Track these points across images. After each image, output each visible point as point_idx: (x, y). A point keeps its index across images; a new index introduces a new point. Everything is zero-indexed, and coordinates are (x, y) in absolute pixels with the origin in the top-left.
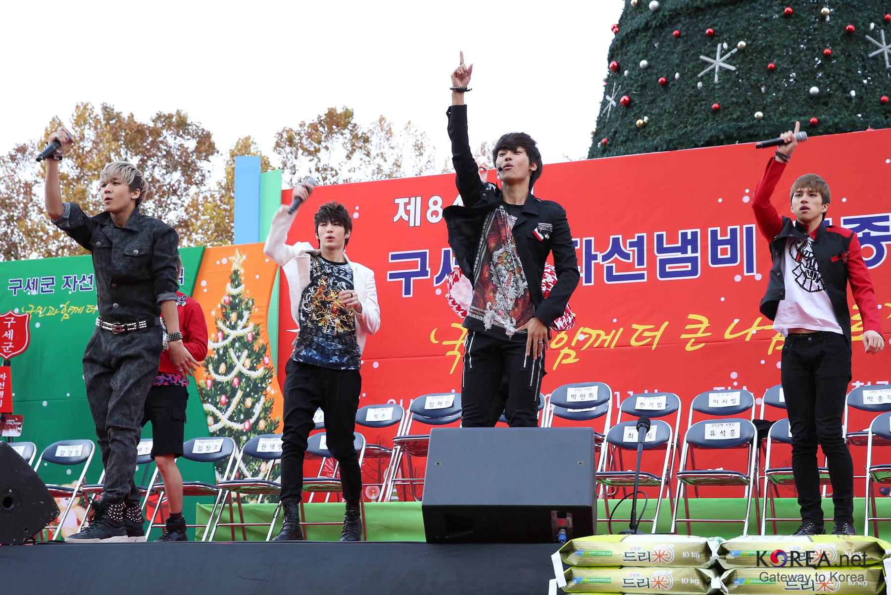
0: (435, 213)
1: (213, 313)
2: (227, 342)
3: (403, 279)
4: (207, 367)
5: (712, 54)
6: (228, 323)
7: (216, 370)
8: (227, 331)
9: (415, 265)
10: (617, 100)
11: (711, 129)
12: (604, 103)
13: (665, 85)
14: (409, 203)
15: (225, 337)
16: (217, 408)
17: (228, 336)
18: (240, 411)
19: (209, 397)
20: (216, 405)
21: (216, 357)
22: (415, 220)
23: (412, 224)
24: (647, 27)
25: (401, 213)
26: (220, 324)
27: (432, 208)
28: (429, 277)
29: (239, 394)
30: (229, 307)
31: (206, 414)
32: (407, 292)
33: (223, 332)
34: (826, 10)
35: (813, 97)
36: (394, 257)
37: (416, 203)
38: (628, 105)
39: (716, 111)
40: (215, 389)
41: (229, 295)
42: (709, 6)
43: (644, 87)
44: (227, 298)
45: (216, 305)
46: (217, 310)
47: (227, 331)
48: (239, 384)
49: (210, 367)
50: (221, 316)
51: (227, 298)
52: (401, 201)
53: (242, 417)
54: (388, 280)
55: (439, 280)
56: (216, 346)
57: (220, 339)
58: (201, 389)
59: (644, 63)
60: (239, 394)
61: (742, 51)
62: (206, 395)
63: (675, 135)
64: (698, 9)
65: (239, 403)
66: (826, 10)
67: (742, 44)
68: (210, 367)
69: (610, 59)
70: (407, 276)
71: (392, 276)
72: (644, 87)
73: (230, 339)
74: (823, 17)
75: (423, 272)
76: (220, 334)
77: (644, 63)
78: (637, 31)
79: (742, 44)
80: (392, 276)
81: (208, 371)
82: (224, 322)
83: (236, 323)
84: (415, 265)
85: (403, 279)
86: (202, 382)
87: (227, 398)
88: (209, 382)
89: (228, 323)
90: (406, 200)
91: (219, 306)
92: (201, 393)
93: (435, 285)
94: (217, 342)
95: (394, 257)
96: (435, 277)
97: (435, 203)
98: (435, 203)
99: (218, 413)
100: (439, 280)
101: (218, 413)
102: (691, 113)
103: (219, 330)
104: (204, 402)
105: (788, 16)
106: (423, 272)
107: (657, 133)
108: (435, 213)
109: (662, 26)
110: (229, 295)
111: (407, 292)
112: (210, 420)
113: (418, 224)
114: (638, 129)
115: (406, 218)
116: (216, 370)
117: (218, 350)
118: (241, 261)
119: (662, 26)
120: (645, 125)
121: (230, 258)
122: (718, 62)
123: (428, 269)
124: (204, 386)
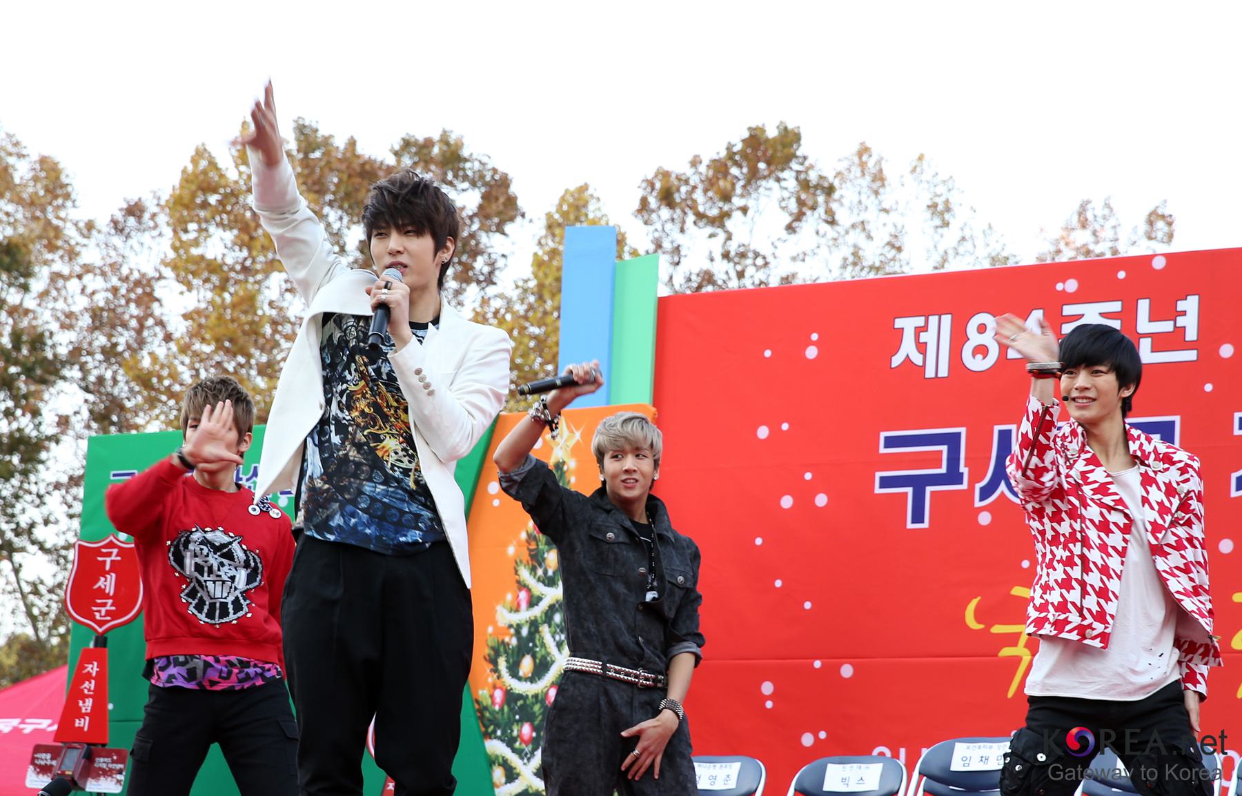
0: (982, 350)
1: (511, 550)
2: (537, 611)
3: (910, 490)
4: (494, 662)
6: (540, 572)
7: (514, 670)
8: (538, 588)
9: (935, 460)
14: (925, 328)
15: (533, 601)
16: (514, 750)
17: (540, 599)
19: (497, 726)
20: (510, 742)
21: (514, 642)
22: (937, 365)
23: (930, 373)
25: (908, 348)
26: (525, 574)
27: (975, 339)
28: (964, 486)
31: (492, 761)
32: (918, 518)
33: (529, 590)
36: (890, 442)
37: (940, 328)
40: (511, 710)
45: (519, 532)
46: (519, 544)
47: (538, 588)
49: (502, 663)
50: (525, 556)
52: (907, 324)
54: (878, 490)
55: (986, 492)
56: (515, 618)
57: (524, 605)
58: (482, 710)
62: (491, 722)
68: (502, 663)
70: (919, 484)
71: (885, 482)
73: (544, 605)
75: (953, 476)
76: (523, 595)
80: (885, 482)
81: (496, 670)
82: (533, 570)
84: (935, 460)
85: (910, 490)
86: (483, 694)
88: (498, 695)
89: (540, 572)
90: (920, 321)
91: (524, 536)
92: (482, 718)
93: (978, 504)
94: (517, 610)
95: (890, 442)
96: (978, 486)
97: (982, 329)
98: (982, 329)
99: (514, 760)
100: (986, 492)
101: (514, 760)
103: (522, 586)
104: (488, 735)
106: (953, 476)
108: (982, 350)
111: (918, 518)
112: (498, 774)
113: (944, 372)
115: (917, 359)
116: (514, 670)
117: (518, 628)
118: (572, 443)
123: (963, 469)
124: (487, 701)
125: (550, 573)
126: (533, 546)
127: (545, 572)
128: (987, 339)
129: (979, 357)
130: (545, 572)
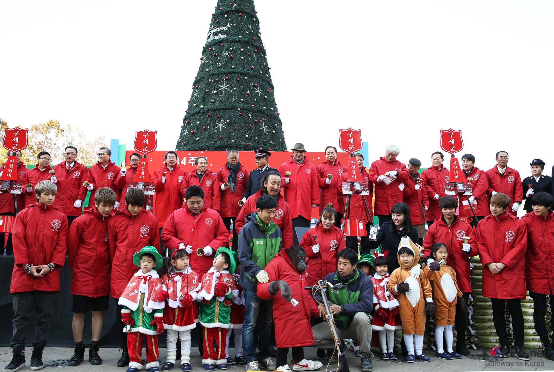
5: (219, 122)
10: (189, 132)
11: (219, 144)
12: (182, 132)
13: (205, 129)
24: (199, 112)
34: (250, 115)
35: (247, 138)
38: (193, 133)
39: (220, 138)
42: (218, 109)
43: (198, 129)
59: (198, 122)
61: (228, 123)
63: (208, 144)
64: (215, 110)
66: (250, 115)
67: (228, 121)
69: (185, 120)
72: (198, 129)
74: (249, 117)
77: (198, 122)
78: (196, 113)
79: (228, 121)
102: (213, 138)
105: (240, 115)
107: (202, 143)
109: (204, 113)
114: (196, 141)
119: (204, 113)
120: (198, 140)
122: (221, 125)
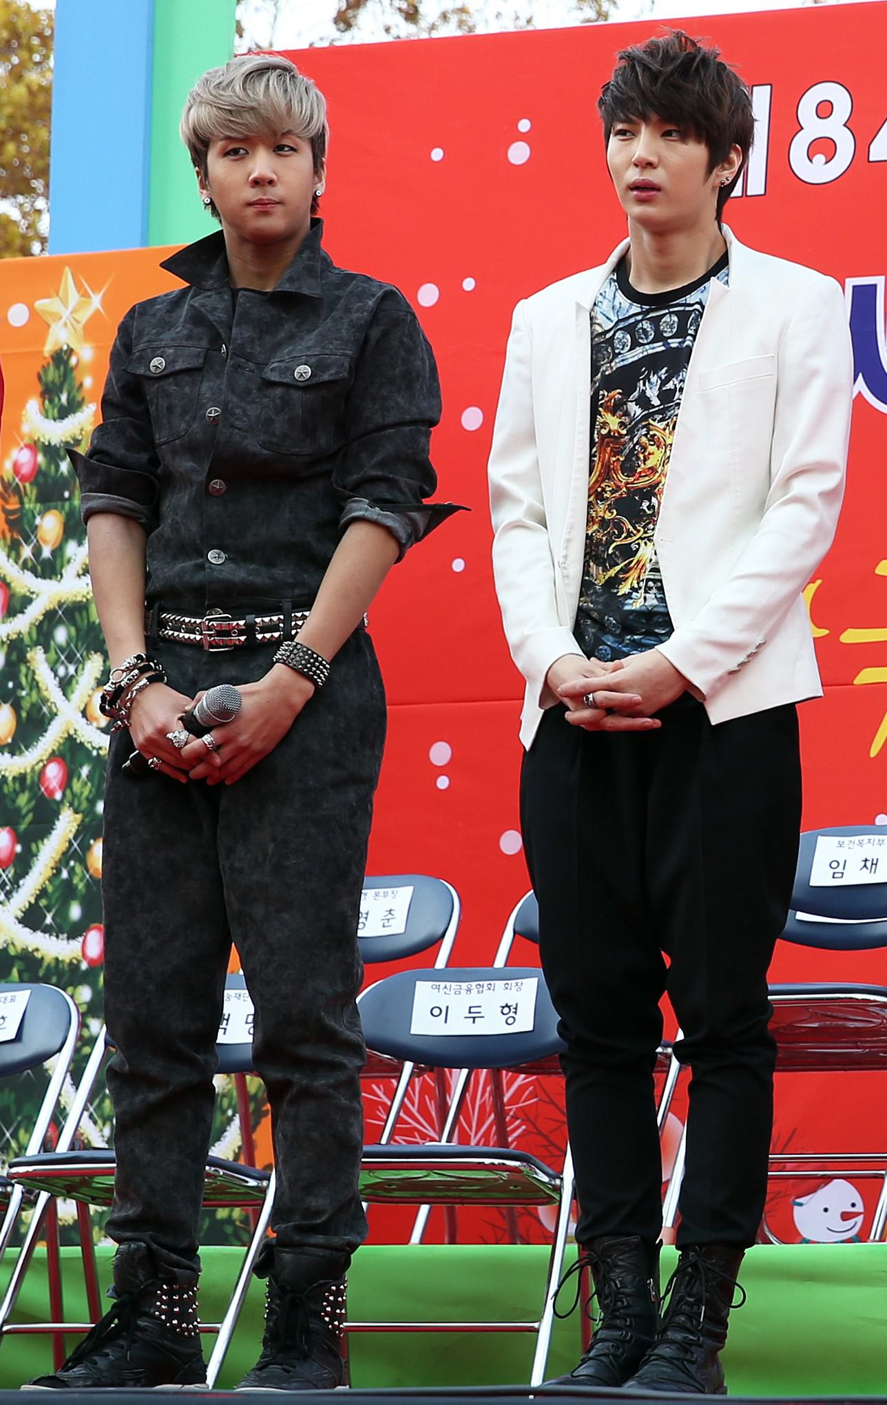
0: (824, 147)
2: (22, 624)
6: (27, 552)
8: (23, 582)
15: (16, 606)
17: (27, 601)
18: (67, 891)
27: (812, 127)
29: (67, 824)
30: (31, 491)
41: (34, 446)
44: (24, 457)
47: (23, 582)
48: (66, 784)
51: (24, 457)
53: (75, 912)
60: (67, 824)
65: (66, 857)
73: (34, 612)
82: (14, 548)
83: (58, 551)
87: (18, 837)
89: (27, 552)
108: (824, 147)
110: (34, 446)
118: (84, 316)
121: (40, 304)
125: (46, 553)
126: (13, 505)
127: (37, 552)
128: (835, 128)
129: (820, 158)
130: (37, 552)
